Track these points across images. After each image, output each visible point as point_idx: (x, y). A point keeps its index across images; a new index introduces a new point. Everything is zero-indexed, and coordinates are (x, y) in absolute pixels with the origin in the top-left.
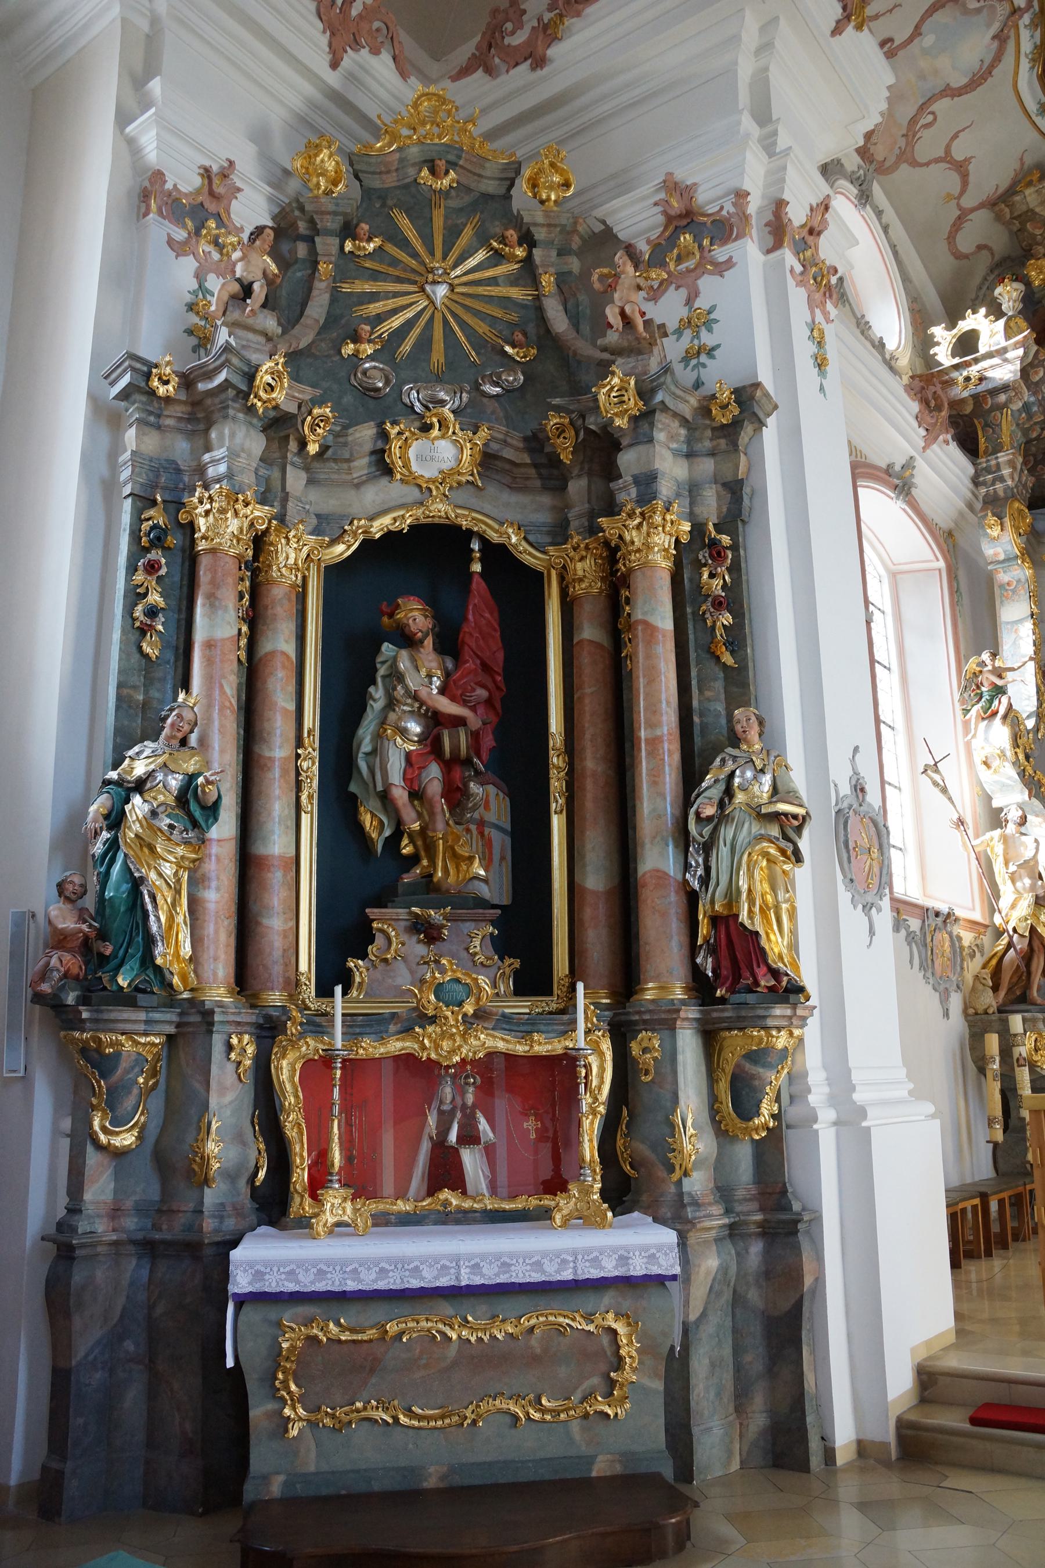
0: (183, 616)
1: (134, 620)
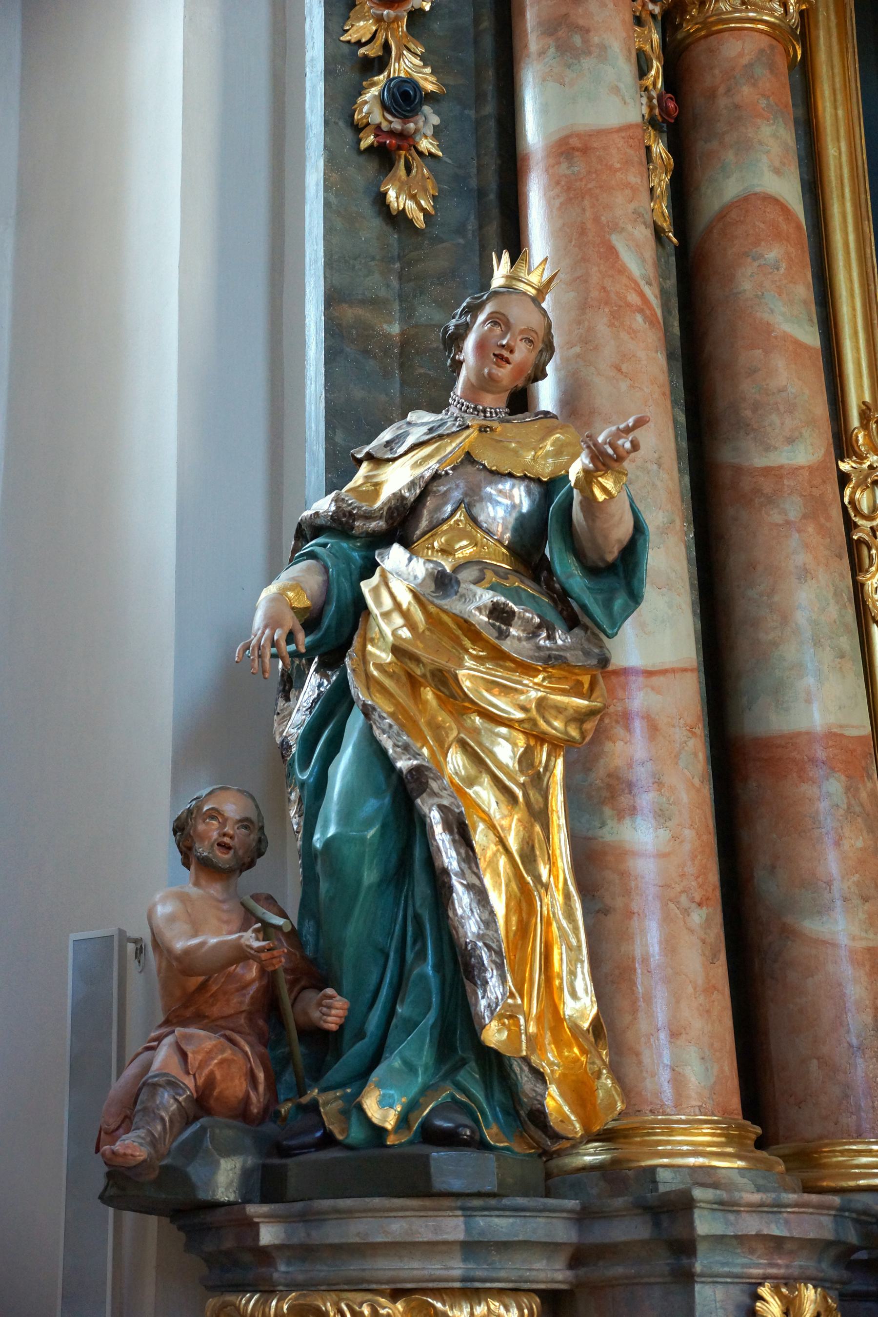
0: (490, 108)
1: (358, 129)
